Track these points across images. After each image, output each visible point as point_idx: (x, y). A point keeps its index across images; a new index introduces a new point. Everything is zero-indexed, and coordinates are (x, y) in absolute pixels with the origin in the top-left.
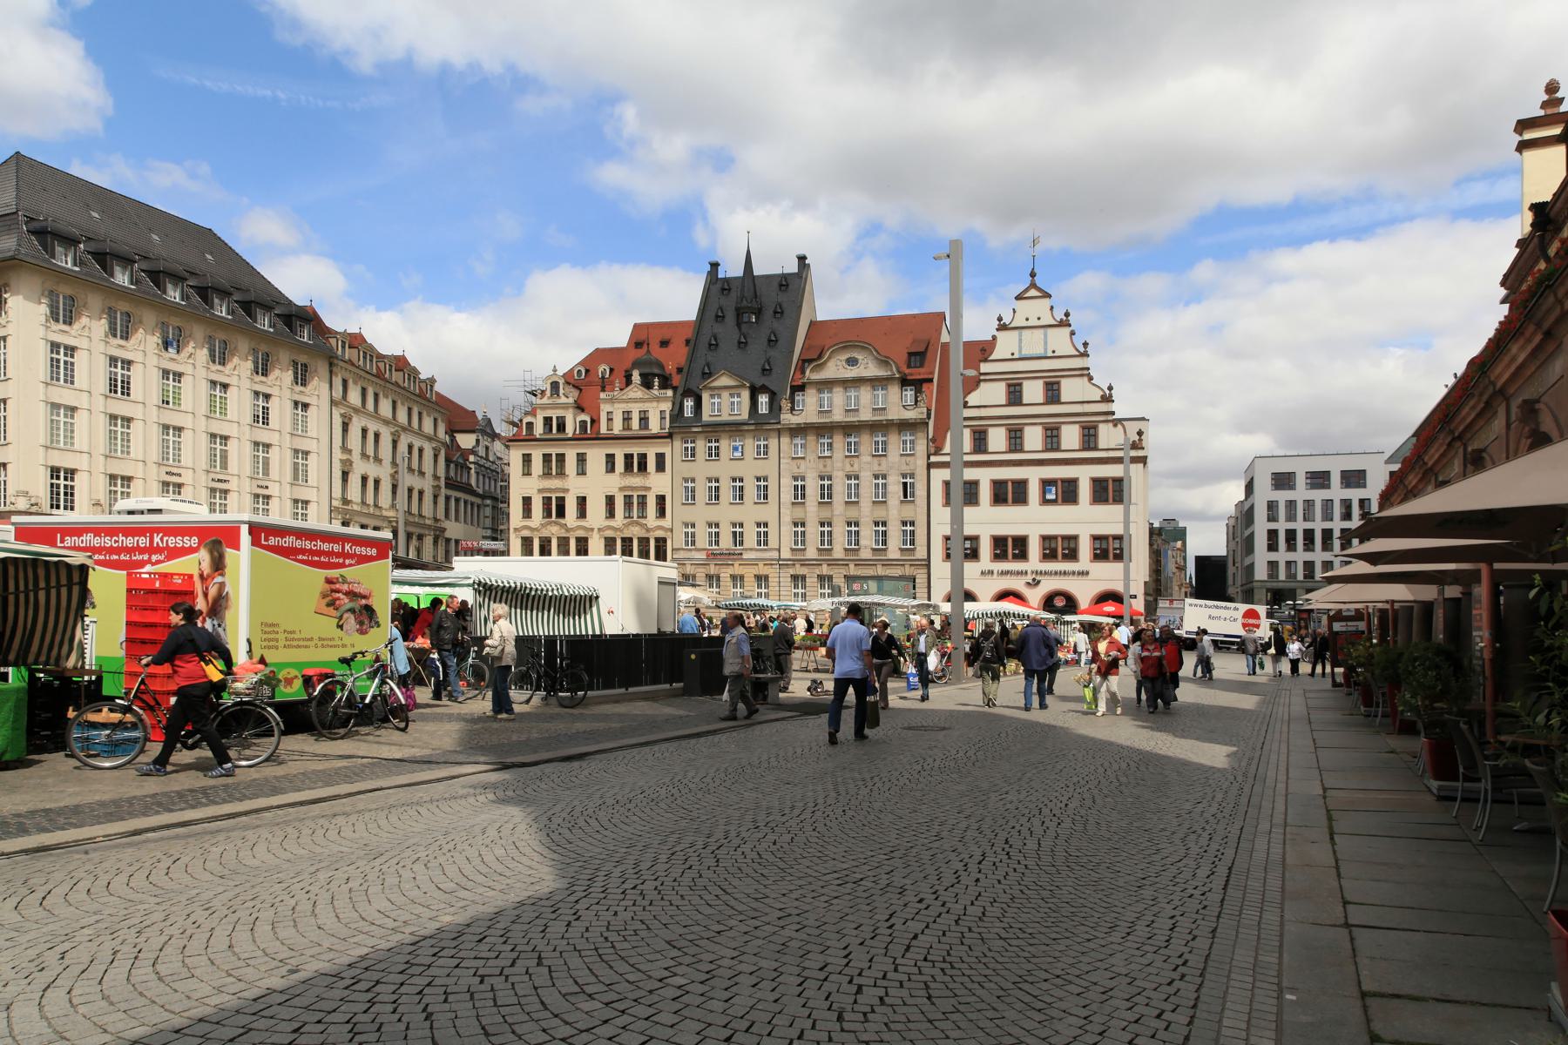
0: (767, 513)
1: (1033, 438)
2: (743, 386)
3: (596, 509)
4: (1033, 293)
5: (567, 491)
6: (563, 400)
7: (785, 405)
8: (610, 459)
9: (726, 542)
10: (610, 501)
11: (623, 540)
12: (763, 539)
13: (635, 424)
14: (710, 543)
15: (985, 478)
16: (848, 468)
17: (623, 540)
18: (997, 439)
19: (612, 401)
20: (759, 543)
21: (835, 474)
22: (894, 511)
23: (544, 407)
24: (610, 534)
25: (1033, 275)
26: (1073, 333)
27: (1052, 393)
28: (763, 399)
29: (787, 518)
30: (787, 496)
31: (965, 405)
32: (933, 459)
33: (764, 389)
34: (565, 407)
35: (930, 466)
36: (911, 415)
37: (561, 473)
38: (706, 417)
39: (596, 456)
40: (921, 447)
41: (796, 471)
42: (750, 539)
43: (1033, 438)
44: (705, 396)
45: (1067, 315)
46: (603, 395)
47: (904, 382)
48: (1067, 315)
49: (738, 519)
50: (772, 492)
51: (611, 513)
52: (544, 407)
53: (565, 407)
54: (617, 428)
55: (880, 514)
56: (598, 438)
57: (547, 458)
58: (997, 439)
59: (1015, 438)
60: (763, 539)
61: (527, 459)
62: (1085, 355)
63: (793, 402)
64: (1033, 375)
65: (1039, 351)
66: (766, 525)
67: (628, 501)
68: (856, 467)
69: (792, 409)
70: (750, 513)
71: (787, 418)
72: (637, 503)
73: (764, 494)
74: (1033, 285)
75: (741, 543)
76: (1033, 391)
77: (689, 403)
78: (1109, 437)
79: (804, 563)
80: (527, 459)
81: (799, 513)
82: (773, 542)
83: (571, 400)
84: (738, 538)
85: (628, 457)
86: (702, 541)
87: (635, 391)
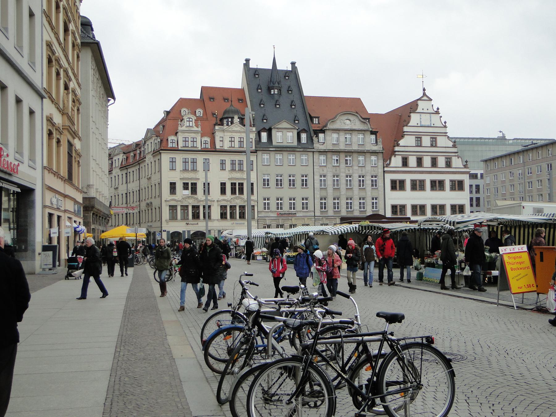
0: (308, 193)
1: (427, 162)
2: (295, 129)
3: (215, 189)
4: (425, 98)
5: (199, 179)
6: (195, 129)
7: (315, 138)
8: (223, 163)
9: (286, 208)
10: (223, 185)
11: (231, 207)
12: (305, 206)
13: (237, 145)
14: (278, 208)
15: (408, 178)
16: (347, 172)
17: (231, 207)
18: (412, 161)
19: (223, 131)
20: (303, 208)
21: (341, 174)
22: (369, 193)
23: (184, 132)
24: (224, 203)
25: (424, 90)
26: (441, 117)
27: (434, 143)
28: (304, 136)
29: (318, 196)
30: (317, 185)
31: (398, 145)
32: (386, 169)
33: (304, 131)
34: (196, 132)
35: (384, 172)
36: (375, 148)
37: (194, 170)
38: (274, 143)
39: (215, 160)
40: (381, 163)
41: (322, 173)
42: (299, 206)
43: (427, 162)
44: (274, 132)
45: (438, 109)
46: (217, 127)
47: (372, 133)
48: (438, 109)
49: (292, 196)
50: (310, 183)
51: (223, 191)
52: (184, 132)
53: (196, 132)
54: (226, 147)
55: (362, 194)
56: (214, 150)
57: (185, 162)
58: (412, 161)
59: (420, 162)
60: (305, 206)
61: (173, 161)
62: (445, 127)
63: (318, 139)
64: (426, 134)
65: (428, 124)
66: (307, 199)
67: (233, 185)
68: (351, 171)
69: (318, 142)
70: (299, 193)
71: (317, 146)
72: (237, 188)
73: (304, 183)
74: (424, 94)
75: (294, 208)
76: (426, 141)
77: (264, 135)
78: (457, 163)
79: (327, 218)
80: (173, 161)
81: (324, 194)
82: (311, 207)
83: (199, 129)
84: (292, 206)
85: (233, 163)
86: (273, 207)
87: (237, 126)
